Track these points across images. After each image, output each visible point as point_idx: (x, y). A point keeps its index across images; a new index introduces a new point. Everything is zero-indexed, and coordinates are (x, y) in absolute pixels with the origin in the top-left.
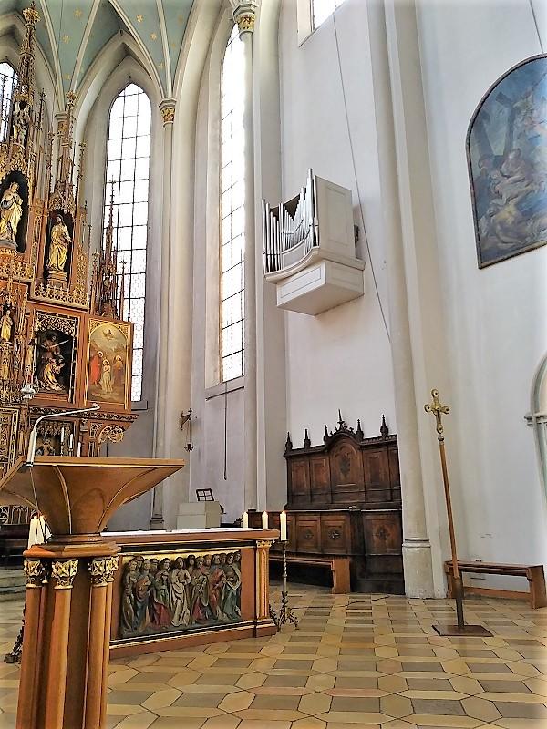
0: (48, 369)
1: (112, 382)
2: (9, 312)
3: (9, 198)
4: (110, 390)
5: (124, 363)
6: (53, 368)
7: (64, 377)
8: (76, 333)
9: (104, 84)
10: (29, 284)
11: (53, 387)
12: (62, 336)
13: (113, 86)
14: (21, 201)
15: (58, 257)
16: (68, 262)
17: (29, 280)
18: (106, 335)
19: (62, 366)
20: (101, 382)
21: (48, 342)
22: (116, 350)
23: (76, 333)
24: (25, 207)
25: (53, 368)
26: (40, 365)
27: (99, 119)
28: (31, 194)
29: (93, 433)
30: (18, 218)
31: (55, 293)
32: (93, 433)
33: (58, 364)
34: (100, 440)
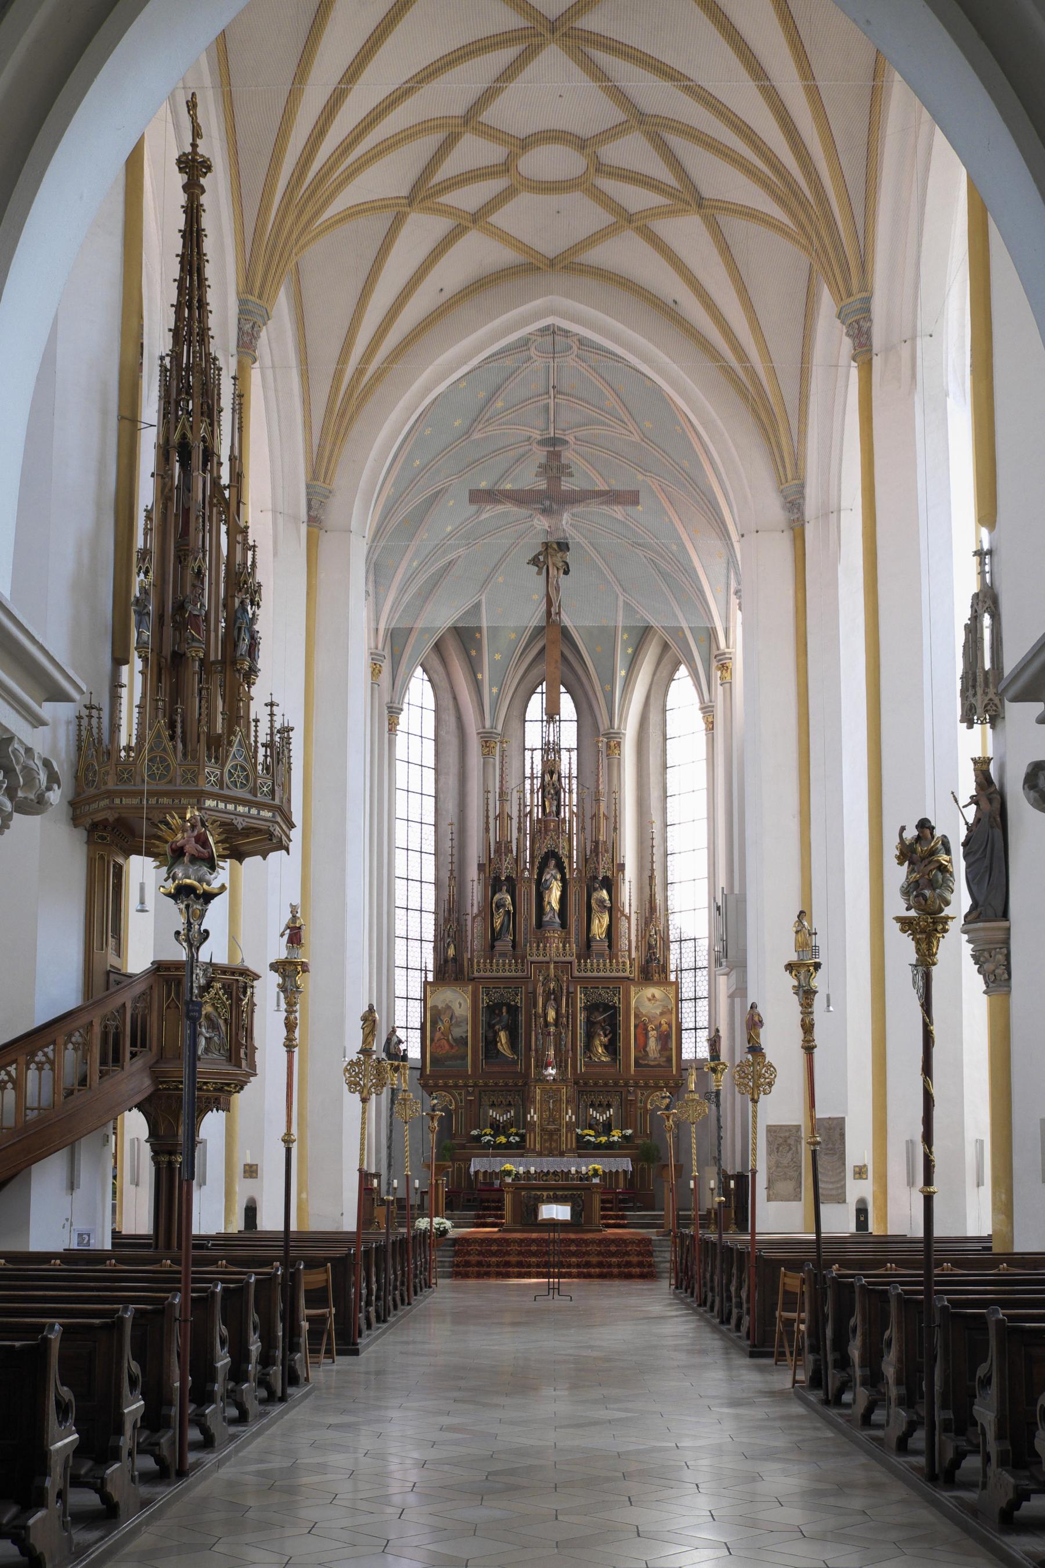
0: (597, 1042)
1: (659, 1047)
2: (553, 997)
3: (548, 877)
4: (657, 1055)
5: (670, 1025)
6: (601, 1041)
7: (612, 1048)
8: (619, 1003)
9: (654, 674)
10: (571, 963)
11: (603, 1059)
12: (606, 1007)
13: (664, 672)
14: (559, 876)
15: (599, 925)
16: (610, 927)
17: (568, 959)
18: (649, 1000)
19: (609, 1036)
20: (648, 1049)
21: (596, 1014)
22: (662, 1014)
23: (619, 1003)
24: (563, 880)
25: (601, 1041)
26: (590, 1037)
27: (654, 717)
28: (567, 867)
29: (641, 1101)
30: (559, 893)
31: (598, 968)
32: (641, 1101)
33: (606, 1036)
34: (649, 1106)
